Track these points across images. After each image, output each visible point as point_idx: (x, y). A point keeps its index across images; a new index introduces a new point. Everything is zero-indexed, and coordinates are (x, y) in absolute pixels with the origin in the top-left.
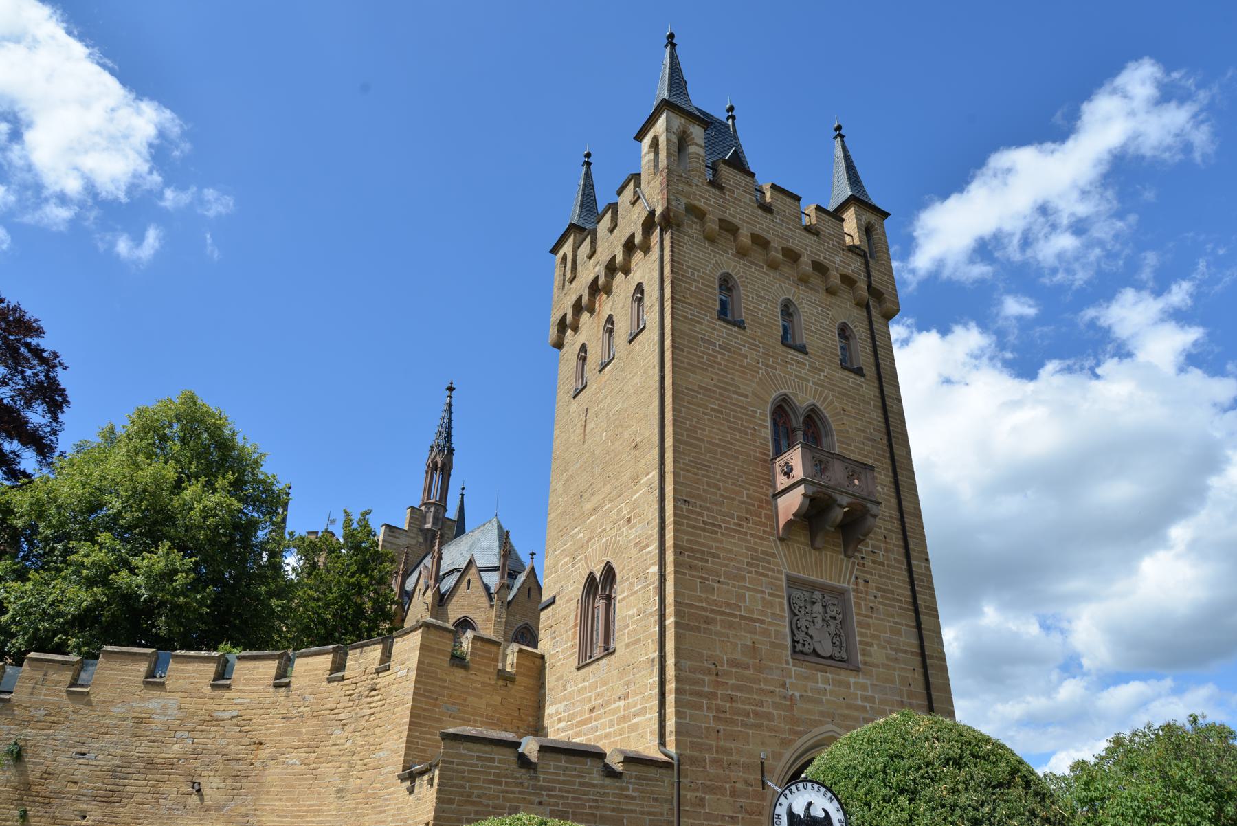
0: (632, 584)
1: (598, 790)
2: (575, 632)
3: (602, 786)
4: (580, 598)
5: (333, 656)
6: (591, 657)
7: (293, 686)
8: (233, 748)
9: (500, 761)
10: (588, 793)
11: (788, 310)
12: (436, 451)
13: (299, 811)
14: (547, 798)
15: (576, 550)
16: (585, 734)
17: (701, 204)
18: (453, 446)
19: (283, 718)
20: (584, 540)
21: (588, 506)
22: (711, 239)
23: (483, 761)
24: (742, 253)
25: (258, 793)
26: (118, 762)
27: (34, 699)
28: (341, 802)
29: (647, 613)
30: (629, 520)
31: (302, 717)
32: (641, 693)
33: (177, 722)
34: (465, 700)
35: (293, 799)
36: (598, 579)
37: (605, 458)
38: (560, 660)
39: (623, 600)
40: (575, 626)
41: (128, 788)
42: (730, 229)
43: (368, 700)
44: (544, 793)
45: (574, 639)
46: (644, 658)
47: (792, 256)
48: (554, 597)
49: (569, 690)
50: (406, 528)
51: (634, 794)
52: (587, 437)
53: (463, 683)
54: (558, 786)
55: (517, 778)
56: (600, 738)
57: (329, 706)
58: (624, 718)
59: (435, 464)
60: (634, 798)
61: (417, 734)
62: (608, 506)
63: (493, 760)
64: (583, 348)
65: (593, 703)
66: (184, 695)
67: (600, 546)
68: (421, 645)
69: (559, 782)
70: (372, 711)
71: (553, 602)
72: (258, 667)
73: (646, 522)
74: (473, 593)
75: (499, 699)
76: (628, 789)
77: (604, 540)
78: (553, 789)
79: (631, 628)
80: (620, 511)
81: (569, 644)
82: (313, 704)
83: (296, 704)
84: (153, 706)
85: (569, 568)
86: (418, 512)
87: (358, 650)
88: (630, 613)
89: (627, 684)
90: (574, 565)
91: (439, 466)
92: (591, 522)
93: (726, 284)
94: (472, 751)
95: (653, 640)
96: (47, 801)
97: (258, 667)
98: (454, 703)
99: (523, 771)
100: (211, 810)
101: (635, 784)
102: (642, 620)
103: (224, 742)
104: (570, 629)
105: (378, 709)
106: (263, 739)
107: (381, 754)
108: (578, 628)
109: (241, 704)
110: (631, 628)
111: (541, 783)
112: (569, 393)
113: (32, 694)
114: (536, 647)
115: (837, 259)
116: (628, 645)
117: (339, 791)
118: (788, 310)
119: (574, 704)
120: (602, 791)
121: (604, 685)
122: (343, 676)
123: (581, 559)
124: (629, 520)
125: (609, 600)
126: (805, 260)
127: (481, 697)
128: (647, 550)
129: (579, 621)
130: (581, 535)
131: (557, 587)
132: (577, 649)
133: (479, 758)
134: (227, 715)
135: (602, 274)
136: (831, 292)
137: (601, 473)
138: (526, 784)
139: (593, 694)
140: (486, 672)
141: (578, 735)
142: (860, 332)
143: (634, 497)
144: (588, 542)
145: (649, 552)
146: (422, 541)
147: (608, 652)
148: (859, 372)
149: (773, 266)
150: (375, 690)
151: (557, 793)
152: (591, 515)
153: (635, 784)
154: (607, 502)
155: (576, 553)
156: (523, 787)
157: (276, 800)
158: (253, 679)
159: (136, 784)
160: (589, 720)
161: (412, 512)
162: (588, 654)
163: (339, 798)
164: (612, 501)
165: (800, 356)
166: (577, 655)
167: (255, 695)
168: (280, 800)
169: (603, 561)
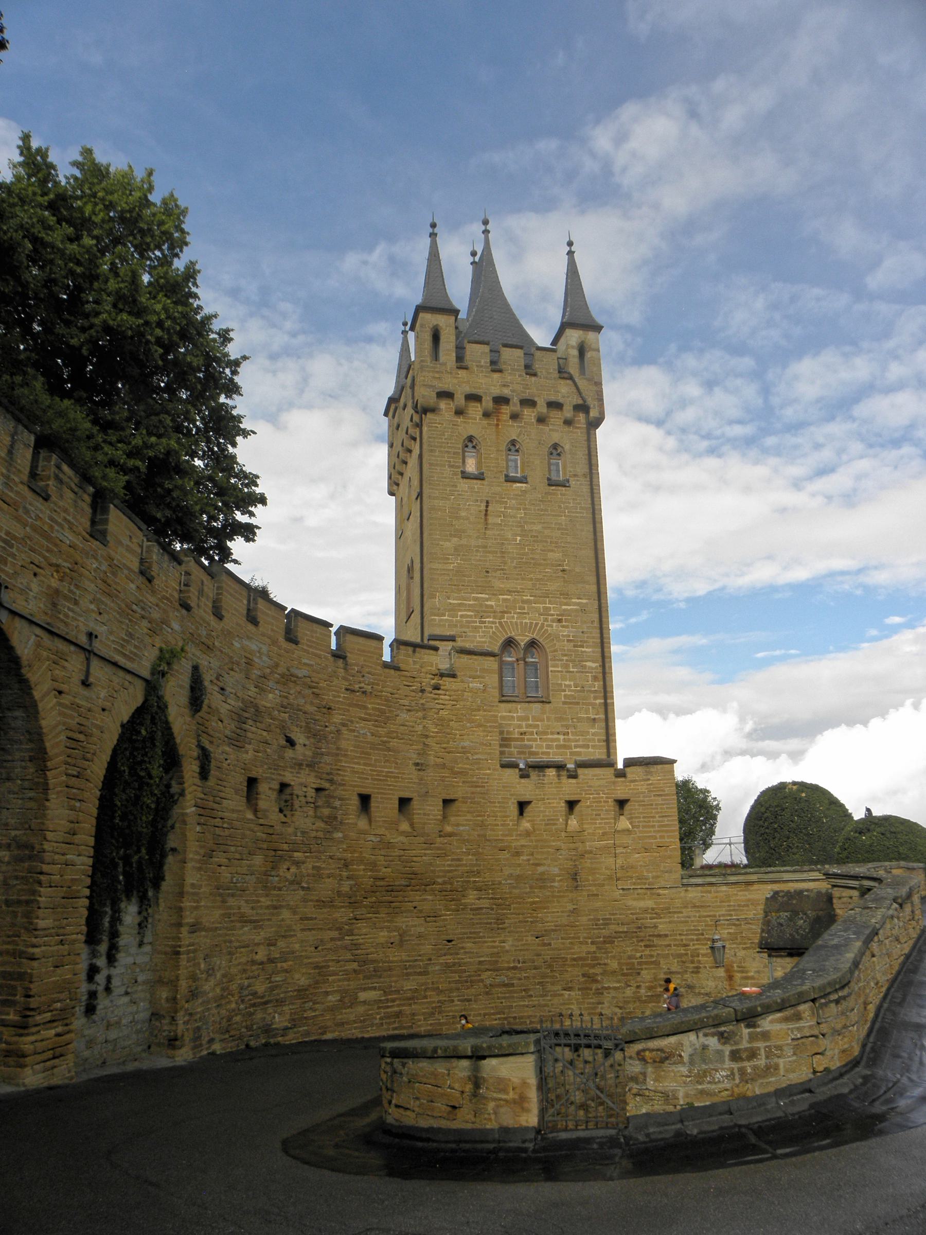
13: (377, 775)
19: (347, 689)
25: (337, 755)
28: (421, 773)
31: (364, 693)
35: (369, 765)
43: (432, 695)
57: (390, 690)
70: (442, 707)
82: (373, 684)
89: (567, 727)
100: (301, 765)
103: (302, 701)
105: (449, 707)
117: (417, 764)
143: (564, 607)
145: (585, 652)
150: (438, 689)
163: (419, 770)
164: (535, 596)
168: (358, 763)
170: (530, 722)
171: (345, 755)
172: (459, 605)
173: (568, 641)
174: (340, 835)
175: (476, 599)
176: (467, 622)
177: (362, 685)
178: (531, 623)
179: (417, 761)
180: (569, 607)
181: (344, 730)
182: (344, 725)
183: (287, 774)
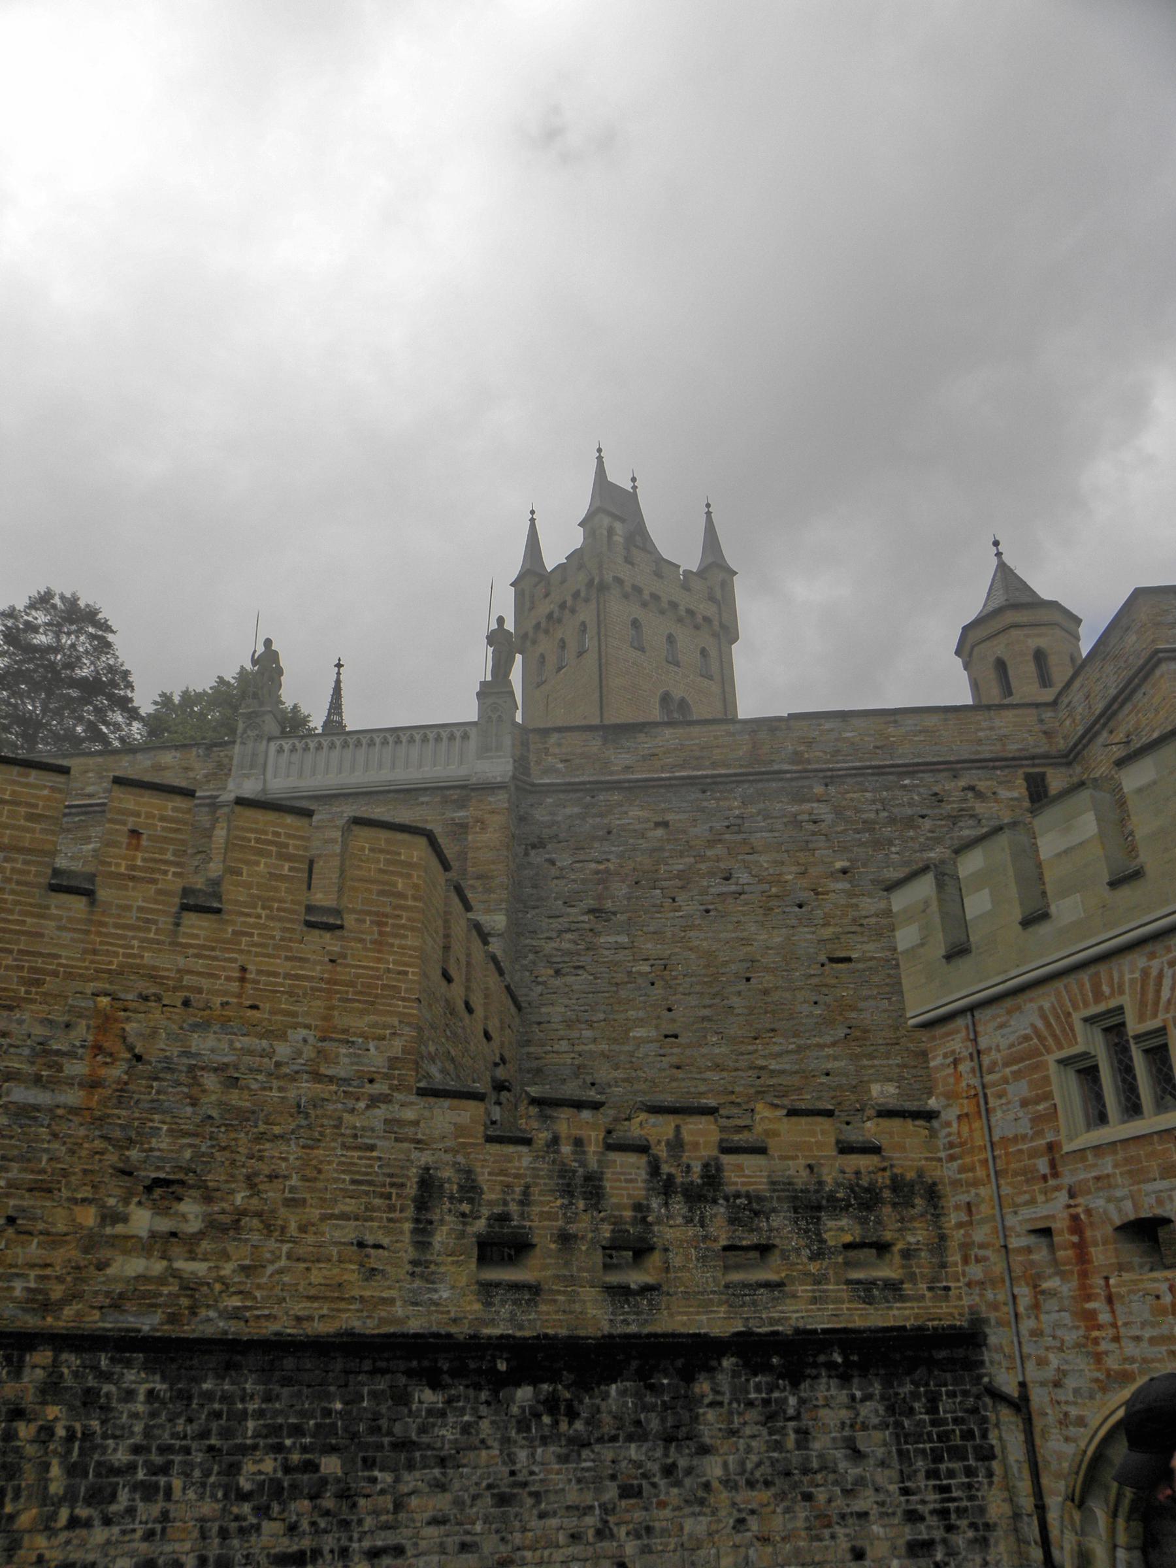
11: (671, 639)
17: (621, 575)
22: (626, 596)
24: (644, 605)
42: (638, 590)
47: (674, 605)
64: (542, 656)
93: (636, 624)
115: (701, 606)
118: (671, 639)
126: (681, 608)
135: (557, 609)
136: (697, 627)
142: (713, 653)
148: (711, 678)
149: (662, 612)
165: (676, 669)
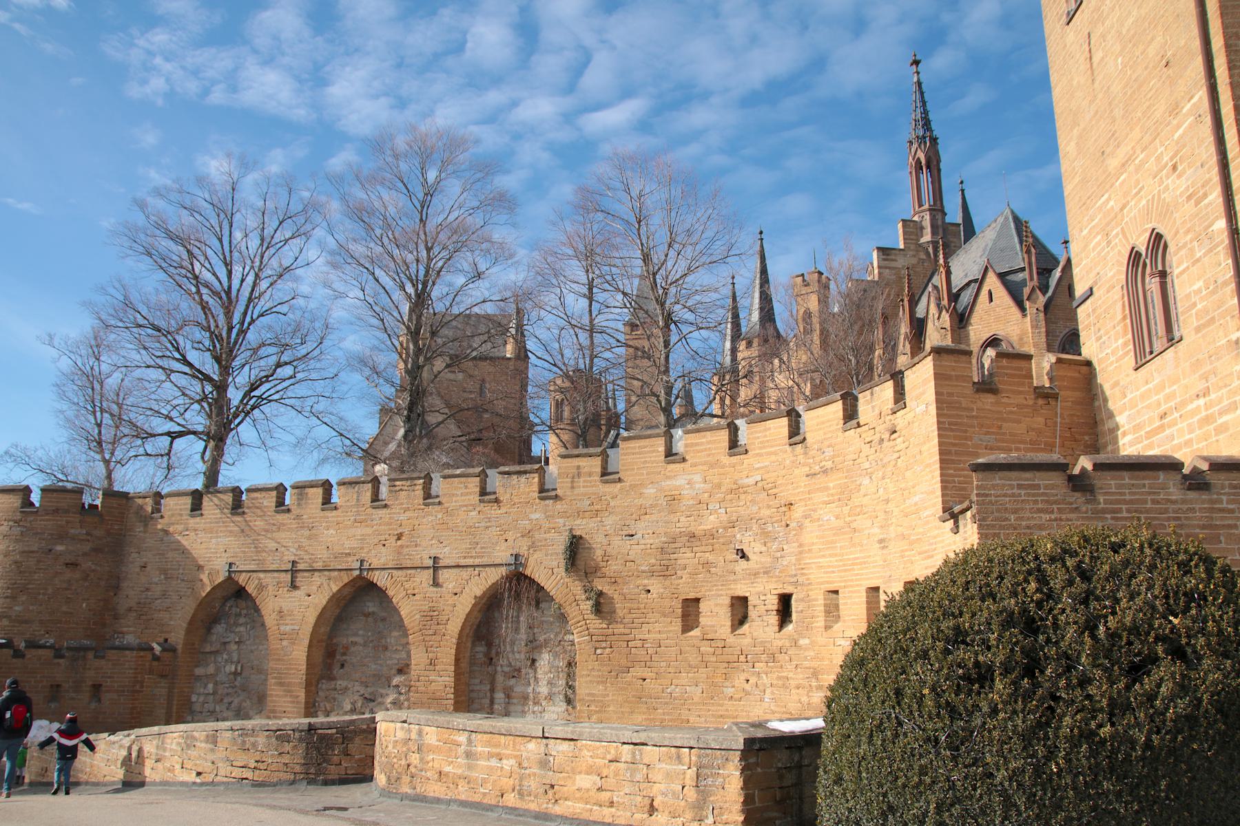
0: (1192, 250)
1: (1180, 506)
2: (1125, 325)
3: (1184, 501)
4: (1124, 283)
5: (843, 404)
6: (1151, 353)
7: (809, 440)
8: (765, 512)
9: (1046, 487)
10: (1166, 511)
12: (915, 146)
13: (844, 565)
14: (1112, 522)
15: (1108, 224)
16: (1159, 446)
18: (934, 133)
20: (1117, 209)
21: (1113, 163)
23: (1026, 489)
26: (664, 539)
27: (576, 491)
29: (1219, 282)
30: (1174, 168)
31: (825, 472)
32: (1226, 386)
33: (706, 495)
34: (1000, 427)
35: (836, 555)
36: (1144, 254)
37: (1125, 94)
38: (1112, 363)
39: (1184, 271)
40: (1124, 318)
41: (679, 562)
44: (1109, 516)
45: (1125, 333)
46: (1224, 341)
48: (1091, 289)
49: (1129, 396)
50: (902, 247)
51: (1230, 506)
52: (1095, 74)
53: (994, 409)
54: (1124, 507)
55: (1072, 504)
56: (1179, 447)
58: (1208, 420)
59: (918, 162)
60: (1232, 511)
61: (952, 472)
62: (1142, 156)
63: (1038, 487)
65: (1163, 408)
66: (705, 468)
67: (1139, 211)
68: (935, 374)
69: (1125, 502)
71: (1091, 294)
72: (770, 429)
73: (1199, 164)
74: (998, 306)
75: (1041, 420)
76: (1221, 502)
77: (1144, 202)
78: (1120, 511)
79: (1199, 306)
80: (1158, 159)
81: (1121, 341)
83: (818, 459)
84: (680, 481)
85: (1103, 249)
86: (912, 224)
87: (868, 392)
88: (1195, 287)
90: (1109, 243)
91: (923, 162)
92: (1121, 184)
94: (1010, 479)
95: (1233, 317)
96: (613, 580)
97: (770, 429)
98: (987, 433)
99: (1077, 494)
100: (758, 573)
101: (1229, 494)
102: (1214, 292)
103: (755, 508)
104: (1118, 324)
106: (792, 499)
107: (916, 499)
108: (1128, 321)
109: (762, 468)
110: (1199, 306)
111: (1102, 506)
112: (1060, 20)
113: (573, 487)
114: (1080, 354)
116: (1198, 329)
117: (881, 541)
119: (1138, 412)
120: (1185, 507)
121: (1174, 384)
122: (858, 423)
123: (1117, 234)
124: (1174, 168)
125: (1163, 274)
127: (1019, 422)
128: (1206, 201)
129: (1127, 311)
130: (1112, 203)
131: (1092, 275)
132: (1131, 347)
133: (1020, 487)
134: (751, 481)
137: (1123, 116)
138: (1084, 509)
139: (1161, 396)
140: (1020, 393)
141: (1151, 446)
143: (1176, 136)
144: (1122, 210)
145: (1210, 204)
146: (924, 257)
147: (1172, 340)
150: (895, 432)
151: (1125, 514)
152: (1122, 174)
153: (1229, 494)
154: (1138, 152)
155: (1108, 228)
156: (1080, 512)
157: (819, 557)
158: (768, 441)
159: (686, 557)
160: (1161, 428)
161: (904, 226)
162: (1148, 350)
163: (883, 548)
166: (1132, 353)
167: (773, 458)
168: (824, 556)
169: (1146, 230)
170: (1167, 391)
171: (810, 550)
172: (1090, 232)
173: (1189, 198)
174: (807, 641)
175: (1100, 208)
176: (1099, 253)
177: (823, 463)
178: (1148, 201)
179: (881, 537)
180: (1181, 131)
181: (807, 522)
182: (806, 517)
183: (739, 586)
